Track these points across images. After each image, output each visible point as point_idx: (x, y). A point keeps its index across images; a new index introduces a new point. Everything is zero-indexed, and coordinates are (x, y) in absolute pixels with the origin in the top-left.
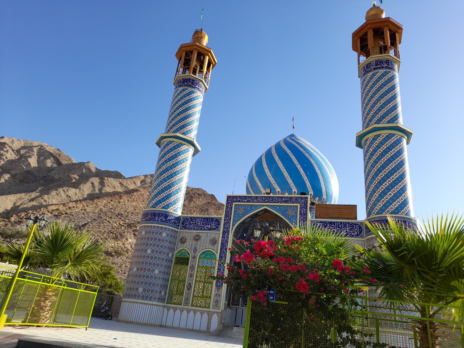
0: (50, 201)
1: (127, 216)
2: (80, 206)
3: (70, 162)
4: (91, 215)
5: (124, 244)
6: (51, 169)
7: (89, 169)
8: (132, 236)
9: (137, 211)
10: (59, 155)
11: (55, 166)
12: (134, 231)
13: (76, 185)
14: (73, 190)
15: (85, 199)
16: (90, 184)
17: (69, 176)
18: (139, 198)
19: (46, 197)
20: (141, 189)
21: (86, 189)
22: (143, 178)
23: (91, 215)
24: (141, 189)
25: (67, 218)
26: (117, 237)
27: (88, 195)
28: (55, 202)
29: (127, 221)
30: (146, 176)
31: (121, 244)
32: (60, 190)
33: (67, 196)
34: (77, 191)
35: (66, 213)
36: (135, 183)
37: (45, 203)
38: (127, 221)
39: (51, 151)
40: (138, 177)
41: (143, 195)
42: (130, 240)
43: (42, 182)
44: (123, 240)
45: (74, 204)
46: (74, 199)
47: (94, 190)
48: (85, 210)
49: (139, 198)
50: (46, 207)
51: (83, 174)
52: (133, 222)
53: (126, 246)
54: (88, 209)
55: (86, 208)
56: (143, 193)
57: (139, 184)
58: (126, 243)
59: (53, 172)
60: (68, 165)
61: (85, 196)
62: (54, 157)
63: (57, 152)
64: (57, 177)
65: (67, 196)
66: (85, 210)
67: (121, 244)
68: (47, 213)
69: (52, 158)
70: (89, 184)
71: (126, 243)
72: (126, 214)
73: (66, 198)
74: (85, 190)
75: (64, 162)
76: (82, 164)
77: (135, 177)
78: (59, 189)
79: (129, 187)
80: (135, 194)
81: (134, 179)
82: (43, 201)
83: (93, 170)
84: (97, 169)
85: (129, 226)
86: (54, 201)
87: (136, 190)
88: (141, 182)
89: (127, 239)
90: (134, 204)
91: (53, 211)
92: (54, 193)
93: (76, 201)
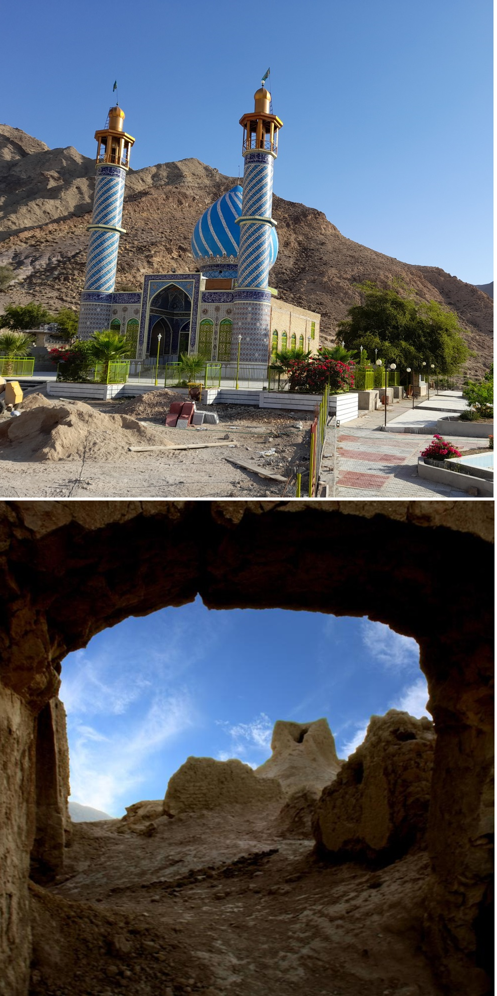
0: (21, 222)
1: (136, 235)
2: (65, 227)
3: (39, 150)
4: (82, 239)
5: (134, 277)
6: (12, 165)
7: (70, 159)
8: (145, 264)
9: (151, 225)
10: (21, 139)
11: (18, 158)
12: (147, 257)
13: (54, 194)
14: (52, 202)
15: (72, 215)
16: (75, 190)
17: (43, 174)
18: (151, 205)
19: (13, 217)
20: (153, 191)
21: (71, 199)
22: (154, 170)
23: (82, 239)
24: (153, 191)
25: (49, 248)
26: (123, 269)
27: (76, 207)
28: (28, 223)
29: (136, 242)
30: (159, 166)
31: (130, 277)
32: (32, 204)
33: (45, 212)
34: (58, 202)
35: (47, 241)
36: (143, 181)
37: (14, 227)
38: (136, 242)
39: (6, 134)
40: (147, 169)
41: (157, 199)
42: (142, 271)
43: (3, 186)
44: (133, 271)
45: (55, 226)
46: (56, 217)
47: (83, 198)
48: (73, 233)
49: (151, 205)
50: (17, 233)
51: (63, 168)
52: (145, 244)
53: (139, 279)
54: (78, 232)
55: (74, 229)
56: (156, 196)
57: (149, 180)
58: (138, 275)
59: (17, 169)
60: (37, 155)
61: (72, 209)
62: (12, 143)
63: (16, 133)
64: (24, 176)
65: (45, 212)
66: (73, 233)
67: (130, 277)
68: (19, 242)
69: (10, 146)
70: (73, 190)
71: (138, 275)
72: (134, 232)
73: (43, 216)
74: (69, 199)
75: (31, 151)
76: (58, 152)
77: (142, 170)
78: (29, 204)
79: (136, 187)
80: (143, 199)
81: (141, 174)
82: (10, 223)
83: (79, 161)
84: (83, 158)
85: (140, 250)
86: (26, 221)
87: (145, 193)
88: (153, 177)
89: (138, 270)
90: (145, 215)
91: (27, 239)
92: (23, 210)
93: (57, 221)
